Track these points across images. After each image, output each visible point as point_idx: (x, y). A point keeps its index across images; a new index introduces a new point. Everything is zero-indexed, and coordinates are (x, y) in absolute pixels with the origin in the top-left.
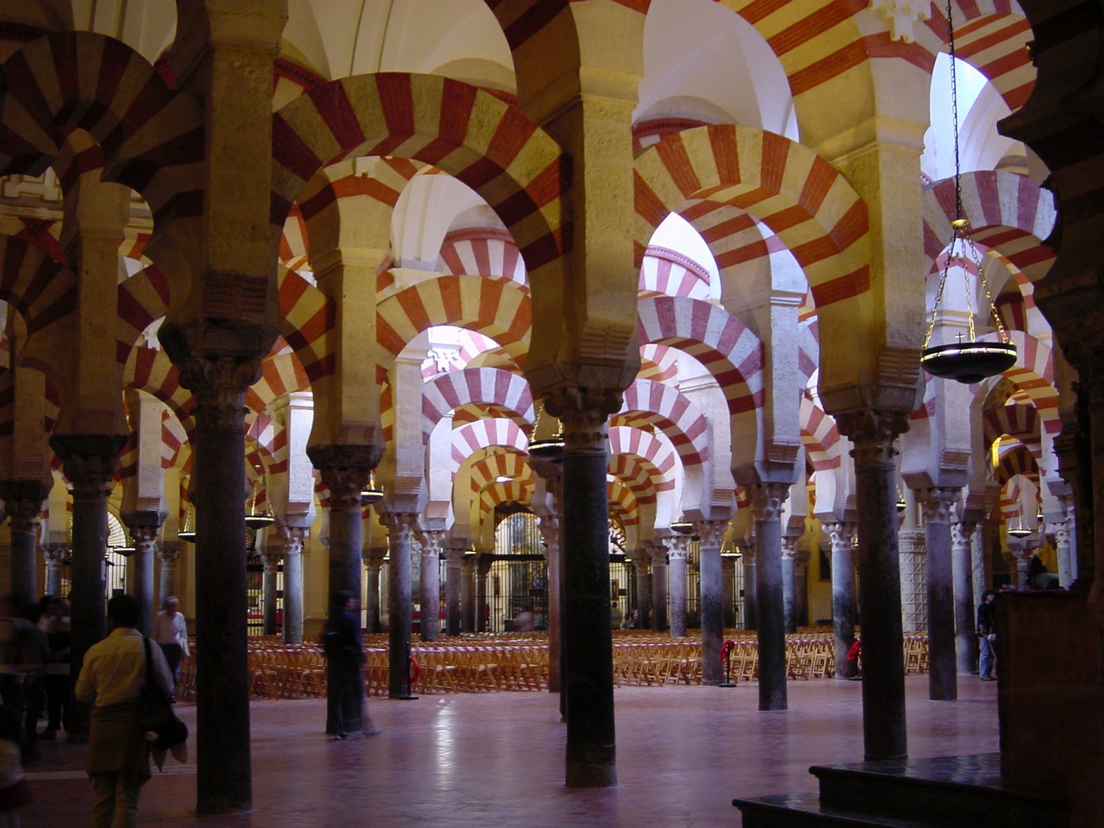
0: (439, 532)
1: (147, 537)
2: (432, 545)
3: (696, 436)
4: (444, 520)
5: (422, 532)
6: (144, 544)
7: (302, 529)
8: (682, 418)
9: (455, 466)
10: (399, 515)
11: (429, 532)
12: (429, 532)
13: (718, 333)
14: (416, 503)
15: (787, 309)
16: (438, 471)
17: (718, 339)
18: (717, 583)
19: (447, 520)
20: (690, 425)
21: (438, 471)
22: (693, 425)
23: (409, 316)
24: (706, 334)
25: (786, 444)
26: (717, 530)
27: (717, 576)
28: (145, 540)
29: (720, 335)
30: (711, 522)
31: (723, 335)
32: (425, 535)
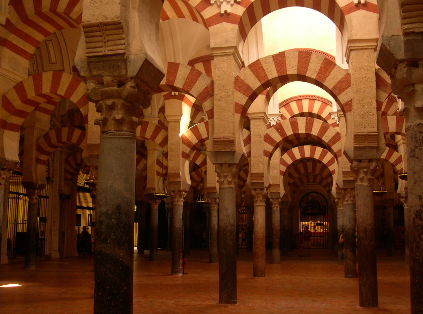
0: (277, 198)
1: (153, 203)
2: (275, 204)
3: (334, 144)
4: (279, 193)
5: (269, 198)
6: (153, 206)
7: (215, 199)
8: (325, 135)
9: (284, 169)
10: (174, 191)
11: (273, 199)
12: (273, 199)
13: (184, 79)
14: (180, 185)
15: (225, 58)
16: (273, 171)
17: (184, 83)
18: (350, 222)
19: (280, 193)
20: (330, 138)
21: (273, 171)
22: (332, 138)
23: (18, 95)
24: (176, 80)
25: (222, 139)
26: (350, 193)
27: (350, 218)
28: (153, 204)
29: (184, 80)
30: (345, 190)
31: (186, 80)
32: (271, 200)
